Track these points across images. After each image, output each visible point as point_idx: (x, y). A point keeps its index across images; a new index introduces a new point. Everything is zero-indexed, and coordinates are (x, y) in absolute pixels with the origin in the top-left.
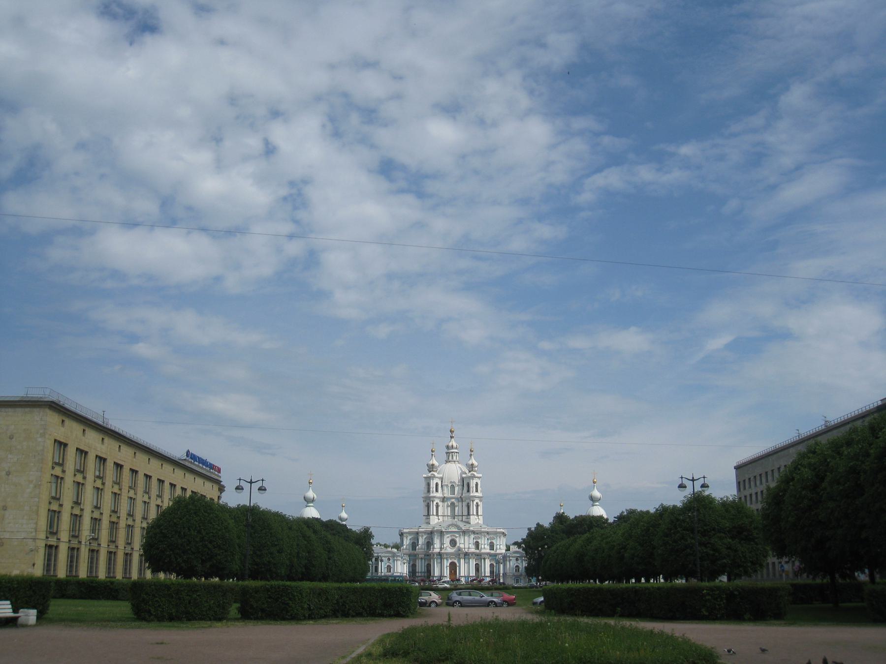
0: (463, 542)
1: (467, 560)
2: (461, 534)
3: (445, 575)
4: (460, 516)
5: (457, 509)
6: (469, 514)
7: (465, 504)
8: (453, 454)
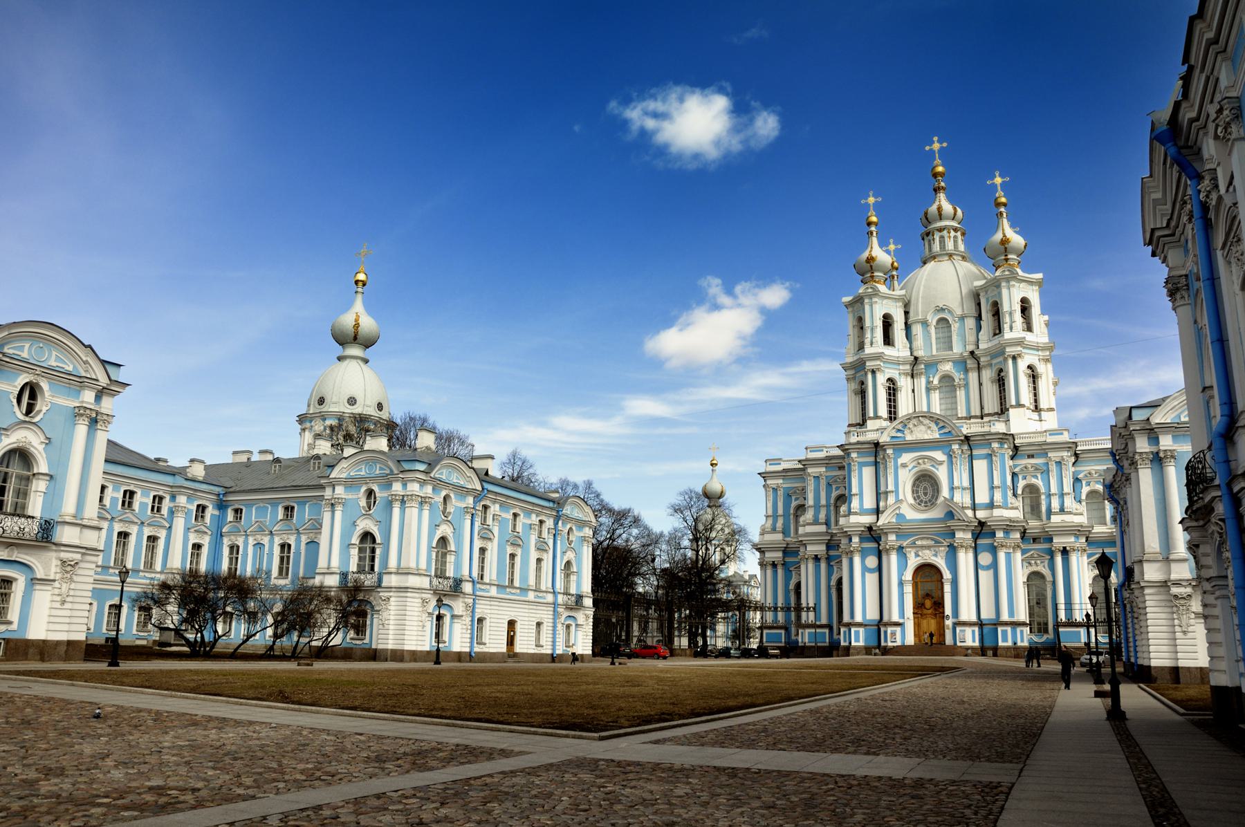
0: (966, 483)
2: (955, 447)
3: (895, 618)
4: (976, 417)
5: (961, 394)
6: (1003, 411)
7: (987, 374)
8: (945, 232)
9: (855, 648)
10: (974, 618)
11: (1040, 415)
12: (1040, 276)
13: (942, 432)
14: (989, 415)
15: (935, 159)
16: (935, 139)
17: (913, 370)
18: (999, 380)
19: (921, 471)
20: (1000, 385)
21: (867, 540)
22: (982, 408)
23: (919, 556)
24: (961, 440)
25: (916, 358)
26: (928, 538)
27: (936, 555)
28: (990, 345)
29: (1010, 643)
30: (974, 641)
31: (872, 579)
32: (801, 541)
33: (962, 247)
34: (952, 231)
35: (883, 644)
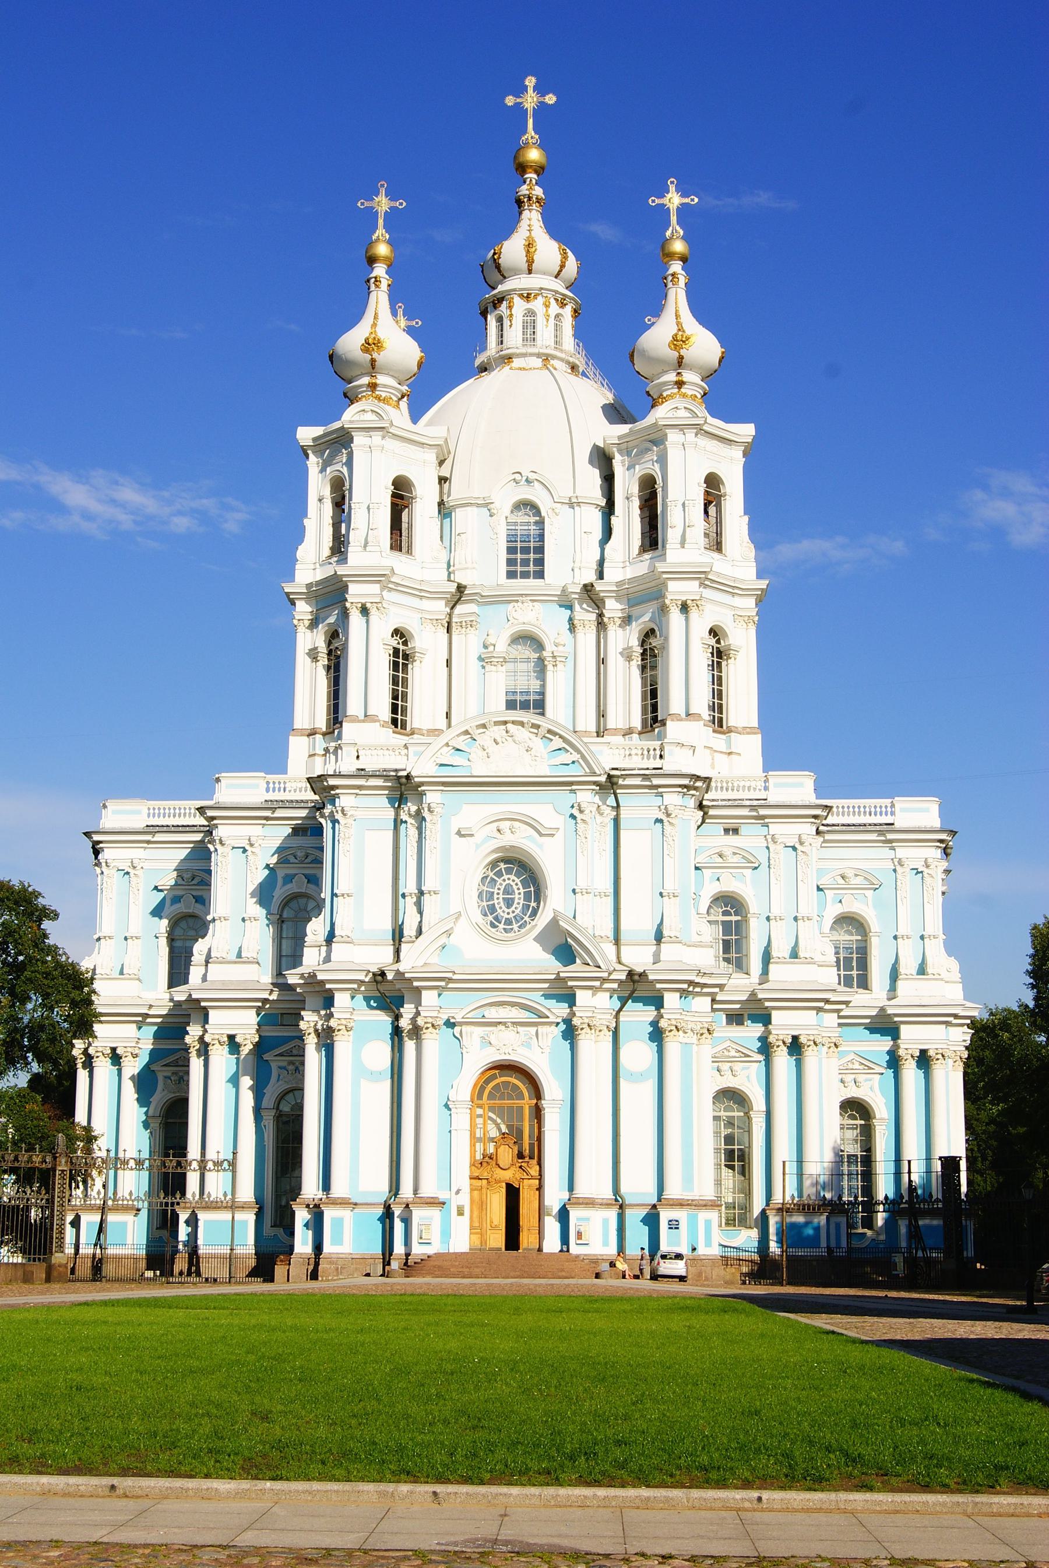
2: (587, 797)
8: (537, 305)
9: (334, 1260)
11: (729, 743)
12: (746, 431)
14: (615, 731)
15: (525, 131)
16: (530, 82)
17: (450, 615)
19: (502, 849)
22: (601, 714)
24: (595, 783)
25: (461, 588)
26: (513, 1004)
27: (527, 1045)
28: (630, 573)
30: (606, 1243)
32: (198, 1001)
33: (569, 342)
34: (552, 301)
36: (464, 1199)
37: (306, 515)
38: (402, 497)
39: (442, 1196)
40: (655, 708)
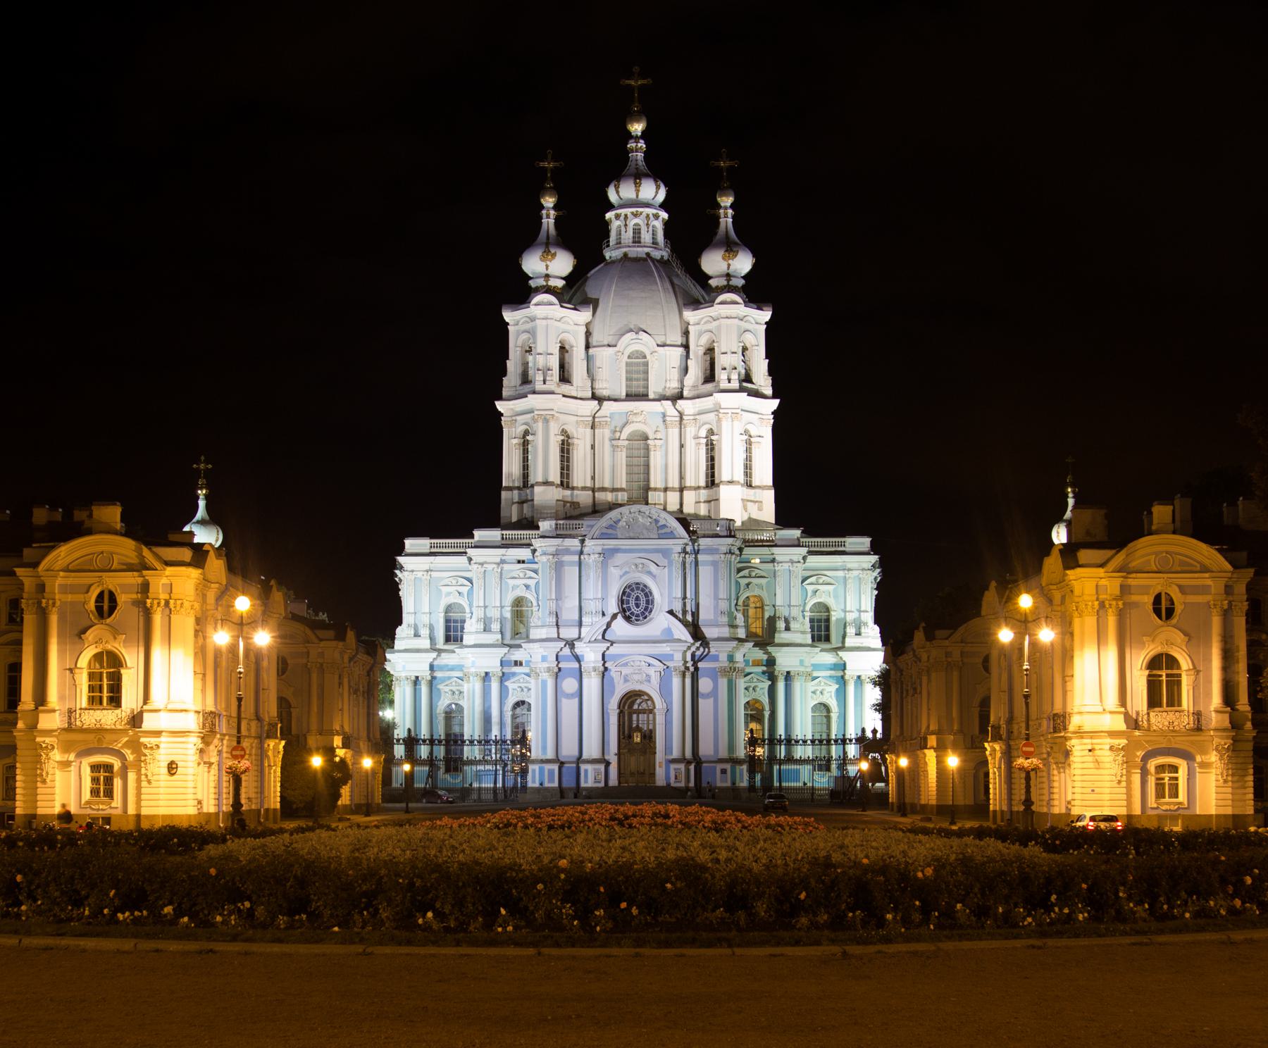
1: (705, 684)
4: (673, 489)
6: (712, 482)
10: (688, 754)
13: (660, 532)
14: (691, 488)
17: (594, 417)
18: (707, 445)
20: (707, 449)
21: (566, 659)
22: (682, 478)
23: (628, 681)
29: (729, 784)
31: (569, 707)
35: (583, 785)
36: (614, 760)
37: (508, 359)
38: (564, 348)
39: (606, 757)
40: (713, 475)
